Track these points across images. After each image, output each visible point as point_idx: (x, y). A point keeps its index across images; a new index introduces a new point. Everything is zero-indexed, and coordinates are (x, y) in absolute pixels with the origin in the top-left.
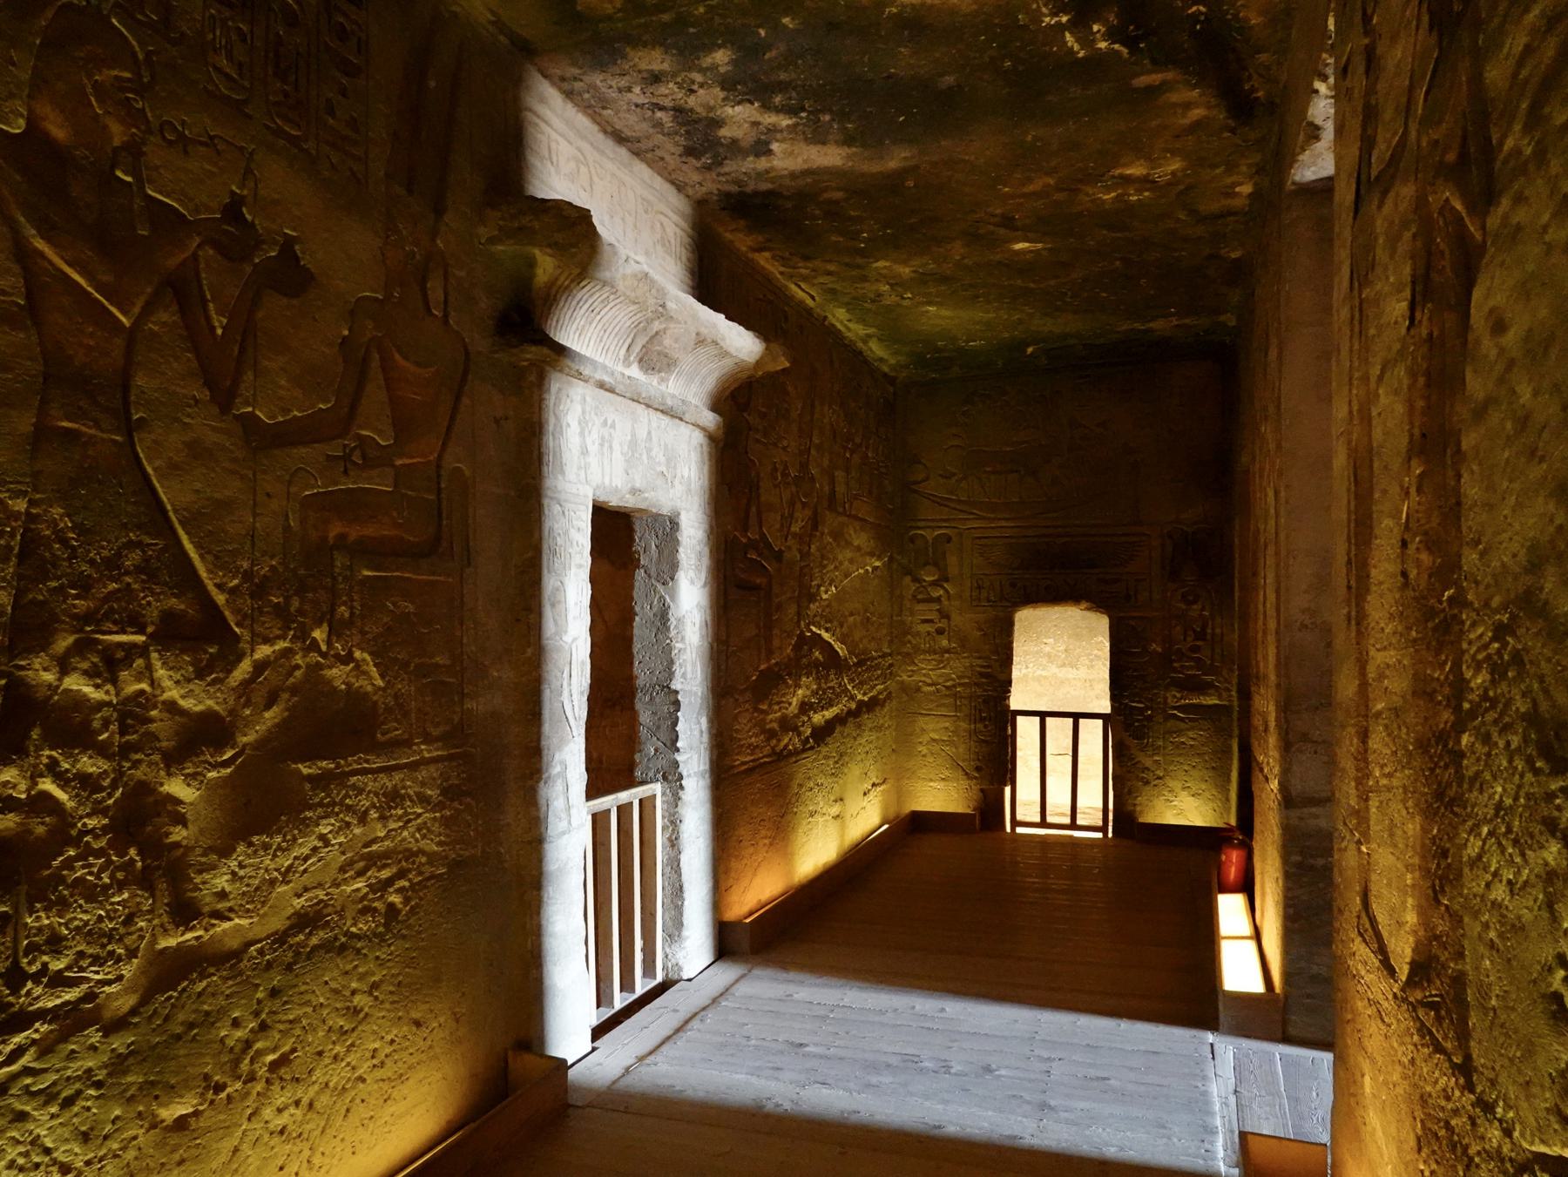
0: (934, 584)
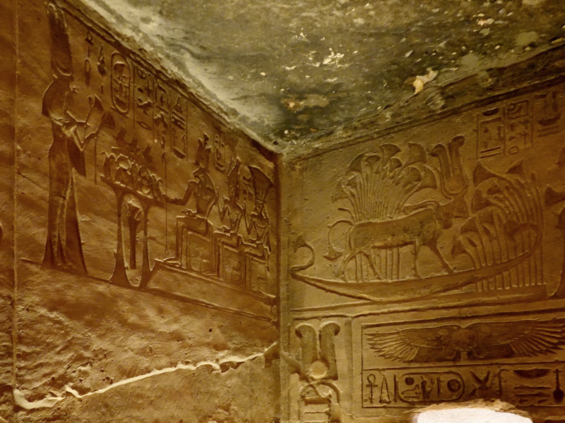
0: (323, 382)
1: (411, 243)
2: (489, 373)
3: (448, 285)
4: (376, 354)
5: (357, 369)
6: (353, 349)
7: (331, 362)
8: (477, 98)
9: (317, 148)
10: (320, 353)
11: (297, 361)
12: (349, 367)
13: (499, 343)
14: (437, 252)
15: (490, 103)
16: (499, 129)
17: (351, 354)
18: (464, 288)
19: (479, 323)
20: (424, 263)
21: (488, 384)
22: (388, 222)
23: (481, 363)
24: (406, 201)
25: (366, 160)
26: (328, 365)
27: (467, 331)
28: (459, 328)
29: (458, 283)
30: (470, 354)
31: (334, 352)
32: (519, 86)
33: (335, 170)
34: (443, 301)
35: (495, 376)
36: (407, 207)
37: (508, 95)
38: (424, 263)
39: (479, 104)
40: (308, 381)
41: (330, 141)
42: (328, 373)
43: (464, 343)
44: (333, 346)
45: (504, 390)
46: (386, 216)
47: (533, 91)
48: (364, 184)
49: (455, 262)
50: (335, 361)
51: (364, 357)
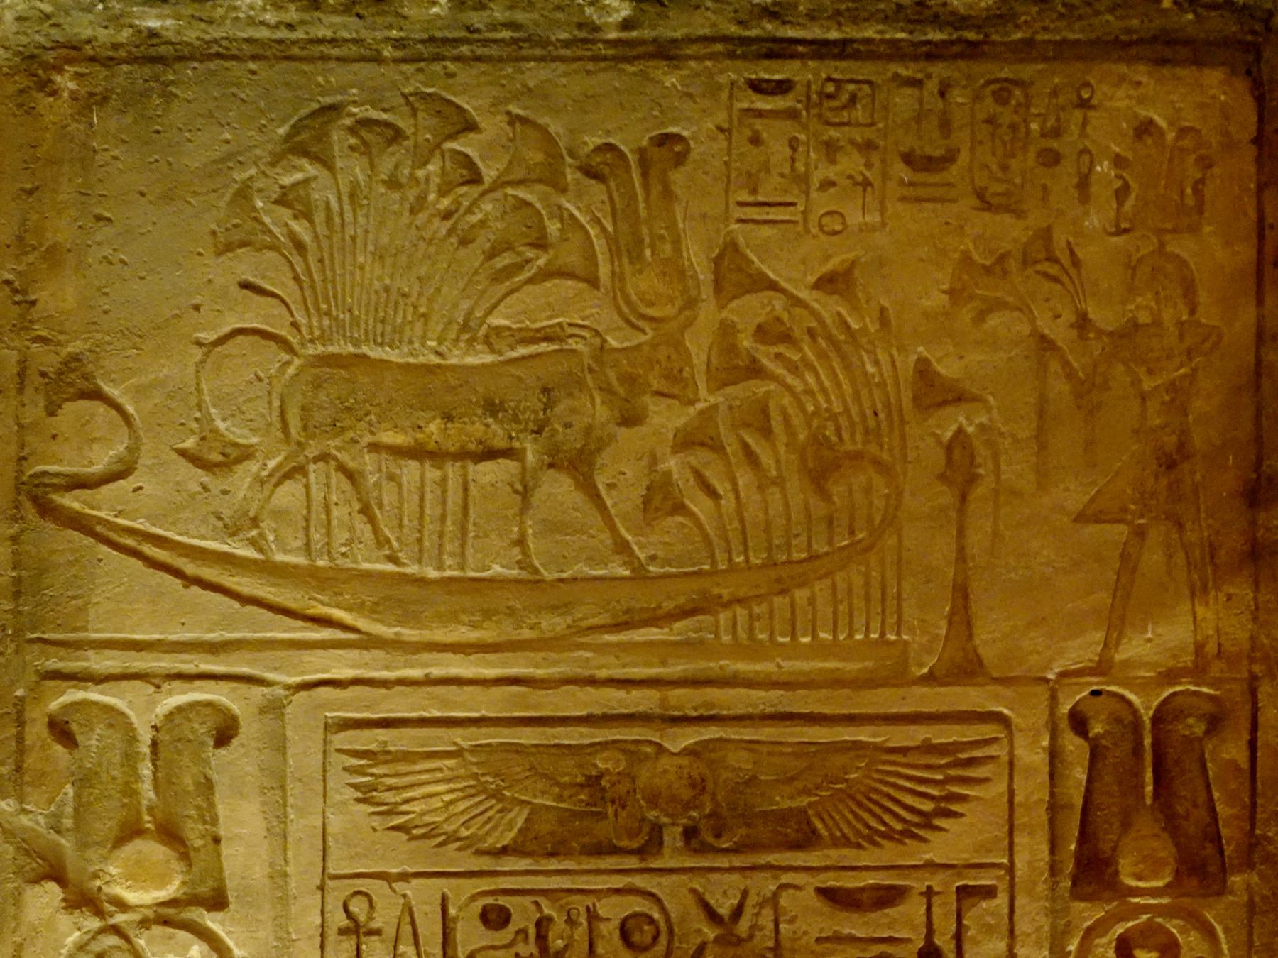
1: (507, 453)
2: (745, 894)
3: (627, 612)
4: (376, 822)
5: (302, 868)
6: (291, 800)
7: (198, 843)
8: (733, 29)
9: (153, 34)
10: (150, 810)
11: (53, 836)
12: (271, 865)
13: (778, 804)
14: (595, 497)
15: (770, 55)
16: (793, 144)
17: (283, 819)
18: (678, 625)
19: (720, 740)
20: (552, 527)
21: (743, 927)
22: (429, 369)
23: (722, 862)
24: (494, 306)
25: (352, 131)
26: (185, 857)
27: (685, 761)
28: (660, 749)
29: (660, 607)
30: (690, 833)
31: (212, 805)
32: (851, 32)
33: (228, 136)
34: (612, 660)
35: (761, 905)
36: (498, 330)
37: (821, 49)
38: (552, 527)
39: (739, 48)
40: (99, 913)
41: (210, 22)
42: (184, 883)
43: (673, 799)
44: (207, 786)
45: (786, 944)
46: (423, 345)
47: (890, 58)
48: (342, 214)
49: (654, 538)
50: (217, 840)
51: (330, 829)
